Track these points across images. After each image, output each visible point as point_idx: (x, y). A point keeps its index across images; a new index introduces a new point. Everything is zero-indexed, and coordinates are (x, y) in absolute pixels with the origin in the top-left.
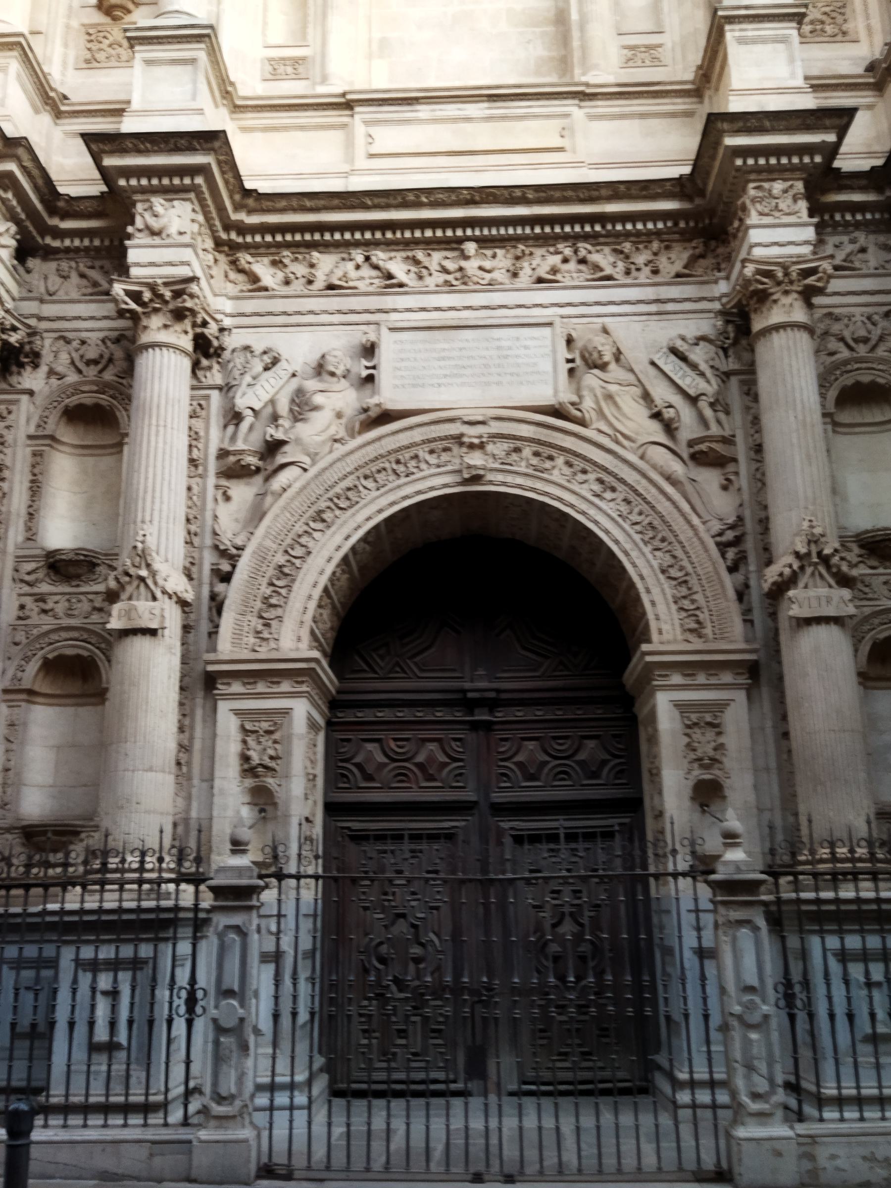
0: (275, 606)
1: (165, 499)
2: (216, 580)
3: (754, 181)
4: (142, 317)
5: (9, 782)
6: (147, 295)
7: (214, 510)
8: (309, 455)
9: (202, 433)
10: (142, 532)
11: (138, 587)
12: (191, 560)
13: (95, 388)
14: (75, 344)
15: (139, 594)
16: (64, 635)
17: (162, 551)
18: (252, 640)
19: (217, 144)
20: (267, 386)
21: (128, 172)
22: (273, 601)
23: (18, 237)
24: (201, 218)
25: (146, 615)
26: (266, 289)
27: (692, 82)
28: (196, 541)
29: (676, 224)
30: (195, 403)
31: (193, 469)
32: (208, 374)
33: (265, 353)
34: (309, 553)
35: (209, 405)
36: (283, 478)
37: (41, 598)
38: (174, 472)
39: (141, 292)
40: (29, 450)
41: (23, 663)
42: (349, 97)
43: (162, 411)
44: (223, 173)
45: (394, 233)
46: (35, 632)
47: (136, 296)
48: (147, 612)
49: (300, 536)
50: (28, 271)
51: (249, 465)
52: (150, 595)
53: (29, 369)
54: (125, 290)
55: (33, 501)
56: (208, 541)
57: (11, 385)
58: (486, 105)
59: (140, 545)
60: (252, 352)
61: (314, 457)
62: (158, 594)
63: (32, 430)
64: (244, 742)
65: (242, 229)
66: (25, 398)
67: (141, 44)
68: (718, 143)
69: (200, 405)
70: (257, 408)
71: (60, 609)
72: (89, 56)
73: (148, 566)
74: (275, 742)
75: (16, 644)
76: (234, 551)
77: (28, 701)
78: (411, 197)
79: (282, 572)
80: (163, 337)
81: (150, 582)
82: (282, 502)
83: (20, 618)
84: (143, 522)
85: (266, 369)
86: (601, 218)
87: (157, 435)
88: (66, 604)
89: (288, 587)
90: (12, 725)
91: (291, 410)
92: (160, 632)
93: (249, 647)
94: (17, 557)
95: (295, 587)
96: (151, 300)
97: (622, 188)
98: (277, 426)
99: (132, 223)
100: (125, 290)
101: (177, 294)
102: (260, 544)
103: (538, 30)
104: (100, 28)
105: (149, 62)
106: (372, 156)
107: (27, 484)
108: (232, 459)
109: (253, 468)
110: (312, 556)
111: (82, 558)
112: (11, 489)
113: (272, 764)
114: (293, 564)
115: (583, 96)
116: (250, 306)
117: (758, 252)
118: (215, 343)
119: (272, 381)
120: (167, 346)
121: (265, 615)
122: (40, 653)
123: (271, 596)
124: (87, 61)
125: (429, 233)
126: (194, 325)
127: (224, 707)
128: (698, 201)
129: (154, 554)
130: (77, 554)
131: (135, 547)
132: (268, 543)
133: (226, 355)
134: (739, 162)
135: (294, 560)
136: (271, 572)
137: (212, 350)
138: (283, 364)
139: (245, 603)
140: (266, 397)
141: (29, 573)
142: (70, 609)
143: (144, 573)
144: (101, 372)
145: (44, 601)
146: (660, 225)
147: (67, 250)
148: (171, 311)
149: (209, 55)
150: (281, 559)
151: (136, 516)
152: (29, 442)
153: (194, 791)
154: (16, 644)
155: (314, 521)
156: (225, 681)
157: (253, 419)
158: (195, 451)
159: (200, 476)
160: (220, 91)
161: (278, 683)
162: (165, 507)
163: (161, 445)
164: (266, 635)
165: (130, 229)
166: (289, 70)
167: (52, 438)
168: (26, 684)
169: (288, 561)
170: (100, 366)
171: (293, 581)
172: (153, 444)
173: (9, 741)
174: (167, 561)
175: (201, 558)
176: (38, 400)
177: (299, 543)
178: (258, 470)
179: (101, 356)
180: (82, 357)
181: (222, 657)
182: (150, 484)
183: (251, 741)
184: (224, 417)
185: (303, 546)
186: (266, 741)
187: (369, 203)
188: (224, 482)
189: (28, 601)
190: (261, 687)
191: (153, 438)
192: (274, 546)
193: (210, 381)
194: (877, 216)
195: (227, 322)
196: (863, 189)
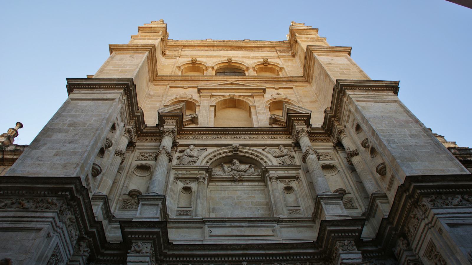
3: (339, 241)
19: (163, 226)
21: (132, 233)
23: (90, 254)
24: (153, 249)
27: (311, 218)
29: (314, 257)
42: (204, 220)
44: (163, 236)
45: (218, 258)
58: (248, 223)
65: (166, 256)
67: (142, 200)
68: (325, 229)
72: (123, 207)
78: (225, 247)
86: (289, 255)
97: (295, 245)
99: (130, 249)
103: (261, 207)
104: (128, 200)
105: (143, 205)
106: (211, 236)
115: (279, 221)
117: (344, 261)
124: (123, 208)
125: (230, 259)
128: (320, 249)
134: (333, 235)
146: (309, 257)
147: (105, 261)
149: (162, 204)
160: (164, 216)
165: (129, 251)
166: (185, 213)
187: (210, 248)
194: (377, 254)
196: (371, 246)
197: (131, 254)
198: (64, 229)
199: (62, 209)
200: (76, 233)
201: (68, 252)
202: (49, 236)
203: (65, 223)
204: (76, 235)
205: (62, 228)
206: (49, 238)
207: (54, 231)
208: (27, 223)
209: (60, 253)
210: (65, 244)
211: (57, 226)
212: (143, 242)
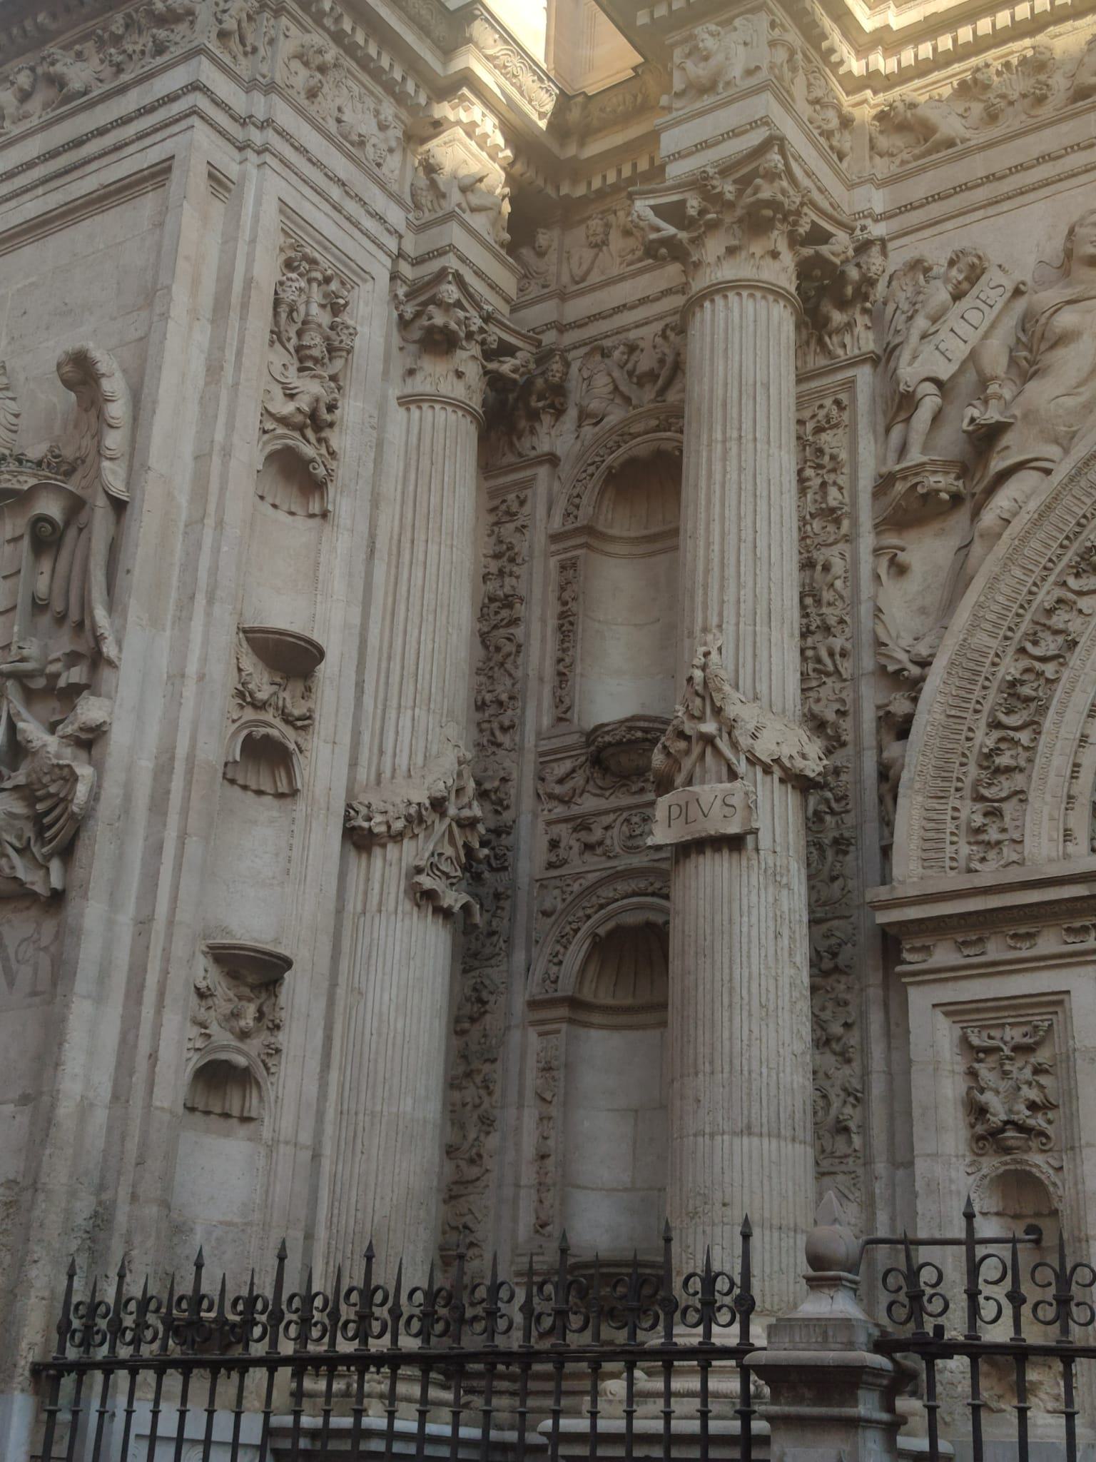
0: (1009, 770)
1: (747, 579)
2: (887, 738)
4: (691, 248)
5: (549, 1180)
6: (693, 204)
7: (874, 598)
8: (1056, 441)
9: (843, 456)
10: (703, 649)
11: (702, 756)
12: (837, 706)
13: (654, 423)
14: (616, 354)
15: (704, 771)
16: (622, 887)
17: (745, 681)
18: (965, 850)
20: (962, 328)
22: (1004, 760)
25: (717, 810)
26: (950, 143)
28: (846, 667)
30: (828, 402)
31: (831, 528)
32: (847, 339)
33: (952, 263)
34: (1075, 643)
35: (854, 399)
36: (1003, 500)
37: (582, 824)
38: (762, 525)
39: (682, 203)
40: (553, 562)
41: (558, 947)
43: (734, 412)
46: (576, 887)
47: (673, 213)
48: (719, 802)
49: (1050, 612)
50: (541, 254)
51: (938, 491)
52: (724, 770)
53: (547, 419)
54: (652, 207)
55: (564, 650)
56: (868, 663)
57: (520, 455)
59: (698, 674)
60: (927, 270)
61: (1066, 442)
62: (742, 767)
63: (557, 524)
64: (972, 1074)
66: (543, 472)
69: (837, 403)
70: (944, 376)
71: (615, 839)
73: (718, 711)
74: (1038, 1070)
75: (546, 914)
76: (915, 671)
77: (571, 1021)
79: (1018, 697)
80: (728, 272)
81: (723, 745)
82: (1001, 548)
83: (551, 866)
84: (705, 630)
85: (957, 297)
87: (724, 459)
88: (625, 828)
89: (1033, 725)
90: (548, 1069)
91: (1013, 361)
92: (750, 839)
93: (962, 863)
94: (542, 754)
95: (1048, 723)
96: (702, 212)
98: (986, 402)
100: (652, 207)
101: (745, 182)
102: (964, 644)
107: (552, 623)
108: (900, 487)
109: (944, 496)
110: (1078, 649)
111: (639, 734)
112: (528, 635)
113: (1039, 1121)
114: (1040, 674)
116: (919, 188)
118: (854, 274)
119: (973, 316)
120: (736, 286)
121: (986, 792)
122: (585, 928)
123: (996, 751)
126: (795, 241)
127: (920, 1000)
129: (727, 688)
130: (630, 729)
131: (690, 679)
132: (981, 639)
133: (880, 289)
135: (1038, 666)
136: (993, 697)
137: (849, 290)
138: (993, 276)
139: (943, 772)
140: (960, 351)
141: (561, 781)
142: (631, 837)
143: (709, 727)
144: (662, 391)
145: (588, 829)
148: (740, 221)
150: (1011, 668)
151: (693, 622)
152: (553, 548)
153: (879, 1188)
154: (546, 914)
155: (1077, 575)
156: (918, 943)
157: (939, 400)
158: (833, 492)
159: (847, 539)
161: (1030, 936)
162: (746, 593)
163: (733, 476)
164: (993, 835)
167: (589, 530)
168: (566, 987)
169: (1027, 671)
170: (660, 382)
171: (1043, 710)
172: (718, 477)
173: (544, 1100)
174: (756, 698)
175: (857, 700)
176: (566, 469)
177: (1049, 628)
178: (957, 499)
179: (662, 361)
180: (630, 374)
181: (900, 892)
182: (715, 556)
183: (986, 1072)
184: (885, 413)
185: (1057, 632)
186: (1021, 1070)
188: (891, 539)
189: (563, 830)
190: (995, 950)
191: (717, 467)
192: (994, 643)
193: (852, 351)
195: (878, 230)
197: (677, 110)
198: (285, 117)
199: (230, 24)
200: (377, 113)
201: (369, 224)
202: (217, 180)
203: (270, 88)
204: (383, 127)
205: (267, 124)
206: (228, 190)
207: (240, 149)
208: (105, 161)
209: (327, 244)
210: (335, 193)
211: (243, 122)
212: (717, 24)
